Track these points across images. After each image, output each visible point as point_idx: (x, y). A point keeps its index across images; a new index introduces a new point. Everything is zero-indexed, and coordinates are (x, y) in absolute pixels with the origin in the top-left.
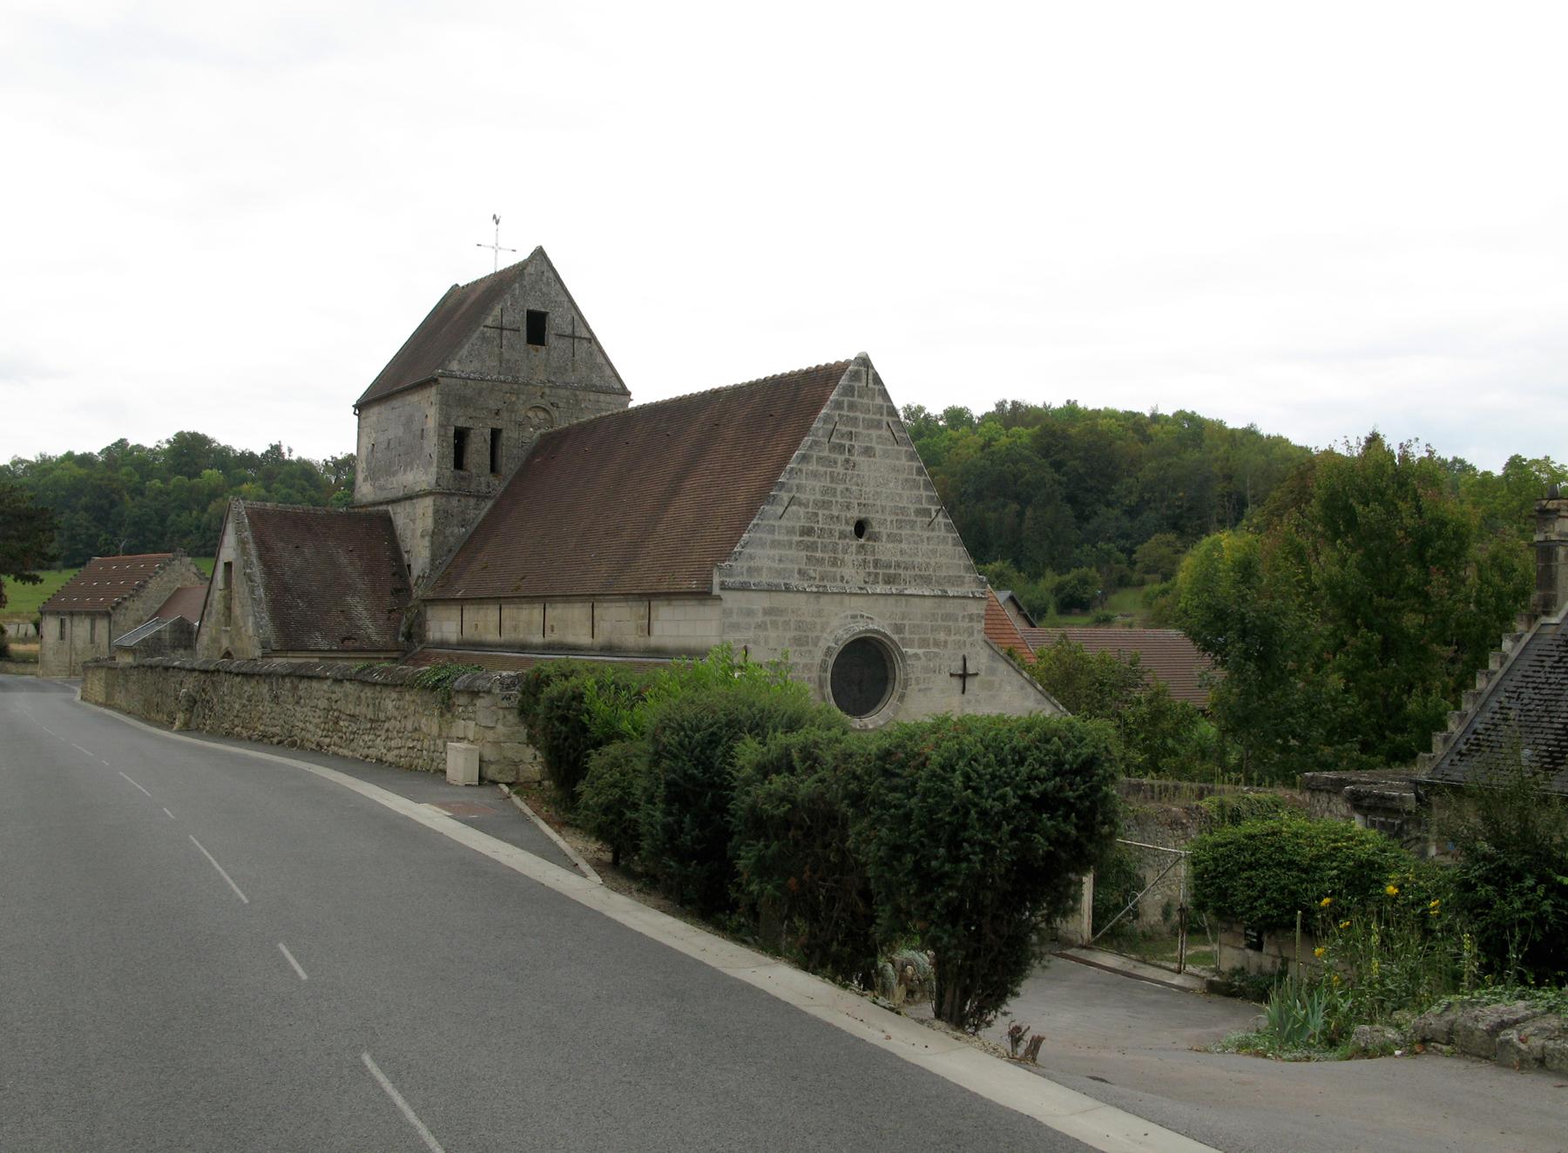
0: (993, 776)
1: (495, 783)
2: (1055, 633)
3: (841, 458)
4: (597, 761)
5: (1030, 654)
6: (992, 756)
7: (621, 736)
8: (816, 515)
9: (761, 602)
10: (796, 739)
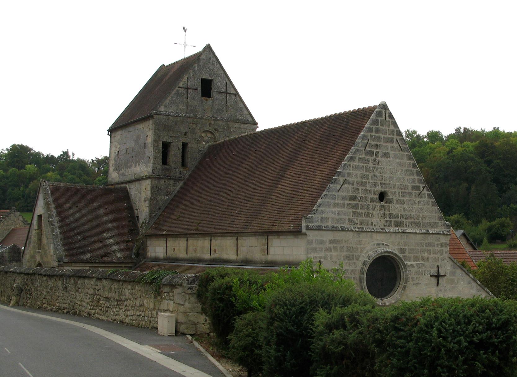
0: (454, 331)
1: (184, 334)
2: (487, 253)
3: (371, 159)
4: (239, 323)
5: (474, 264)
6: (453, 320)
7: (252, 309)
8: (358, 189)
9: (328, 236)
10: (347, 310)
